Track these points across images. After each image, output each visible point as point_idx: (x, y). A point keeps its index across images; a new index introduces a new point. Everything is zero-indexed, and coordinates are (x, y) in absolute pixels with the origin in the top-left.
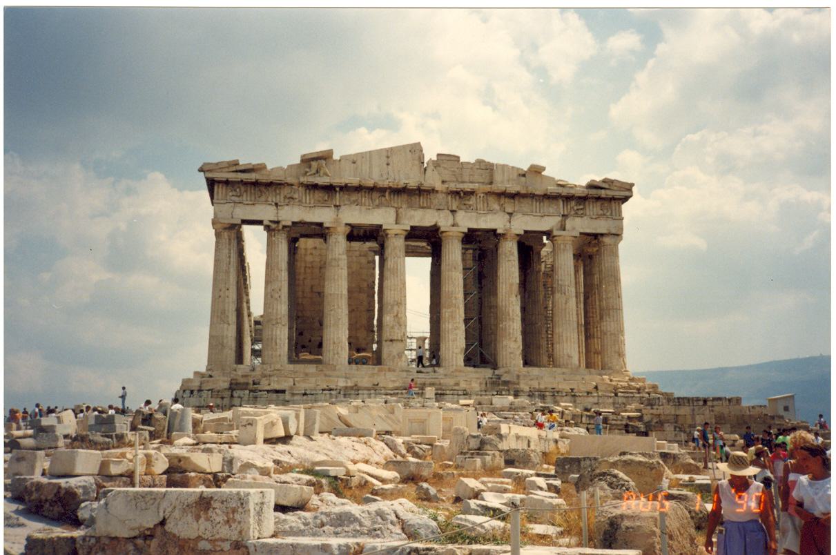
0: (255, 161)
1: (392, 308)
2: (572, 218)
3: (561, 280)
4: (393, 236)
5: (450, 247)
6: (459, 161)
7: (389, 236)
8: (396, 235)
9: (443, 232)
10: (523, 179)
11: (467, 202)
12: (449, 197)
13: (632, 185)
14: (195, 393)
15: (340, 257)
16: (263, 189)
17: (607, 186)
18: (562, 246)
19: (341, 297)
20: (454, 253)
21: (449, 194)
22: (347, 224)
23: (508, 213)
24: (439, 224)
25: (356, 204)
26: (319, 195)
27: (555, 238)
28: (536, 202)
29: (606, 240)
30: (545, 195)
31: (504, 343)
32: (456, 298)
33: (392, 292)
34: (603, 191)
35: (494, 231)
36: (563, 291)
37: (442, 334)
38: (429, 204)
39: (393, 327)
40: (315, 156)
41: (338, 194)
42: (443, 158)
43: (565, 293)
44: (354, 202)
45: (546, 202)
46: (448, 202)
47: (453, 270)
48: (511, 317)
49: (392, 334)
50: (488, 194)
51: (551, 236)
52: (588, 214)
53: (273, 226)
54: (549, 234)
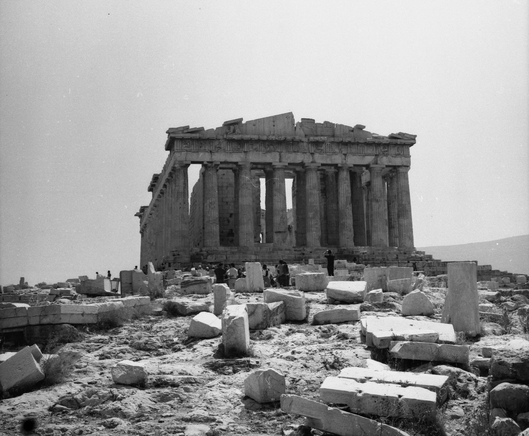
0: (198, 126)
10: (352, 133)
11: (320, 148)
13: (415, 136)
14: (172, 264)
16: (202, 142)
24: (305, 162)
26: (235, 145)
30: (365, 143)
40: (233, 122)
42: (305, 121)
44: (255, 149)
46: (309, 148)
50: (333, 142)
53: (210, 165)
54: (367, 166)
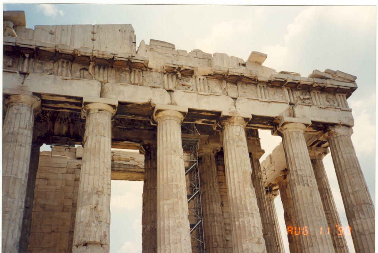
1: (89, 199)
2: (300, 106)
3: (300, 170)
4: (97, 111)
5: (168, 128)
6: (174, 48)
7: (91, 112)
8: (100, 110)
9: (159, 111)
12: (166, 76)
15: (21, 131)
17: (330, 77)
18: (295, 134)
19: (14, 183)
20: (170, 138)
21: (165, 74)
22: (35, 94)
23: (233, 98)
24: (154, 102)
25: (49, 72)
27: (285, 127)
28: (261, 89)
29: (340, 131)
31: (245, 246)
32: (177, 187)
33: (91, 177)
34: (328, 81)
35: (219, 113)
36: (305, 182)
37: (160, 235)
38: (141, 81)
39: (88, 225)
41: (26, 61)
43: (308, 185)
45: (271, 91)
47: (173, 152)
48: (249, 211)
49: (87, 233)
51: (280, 125)
52: (315, 103)
